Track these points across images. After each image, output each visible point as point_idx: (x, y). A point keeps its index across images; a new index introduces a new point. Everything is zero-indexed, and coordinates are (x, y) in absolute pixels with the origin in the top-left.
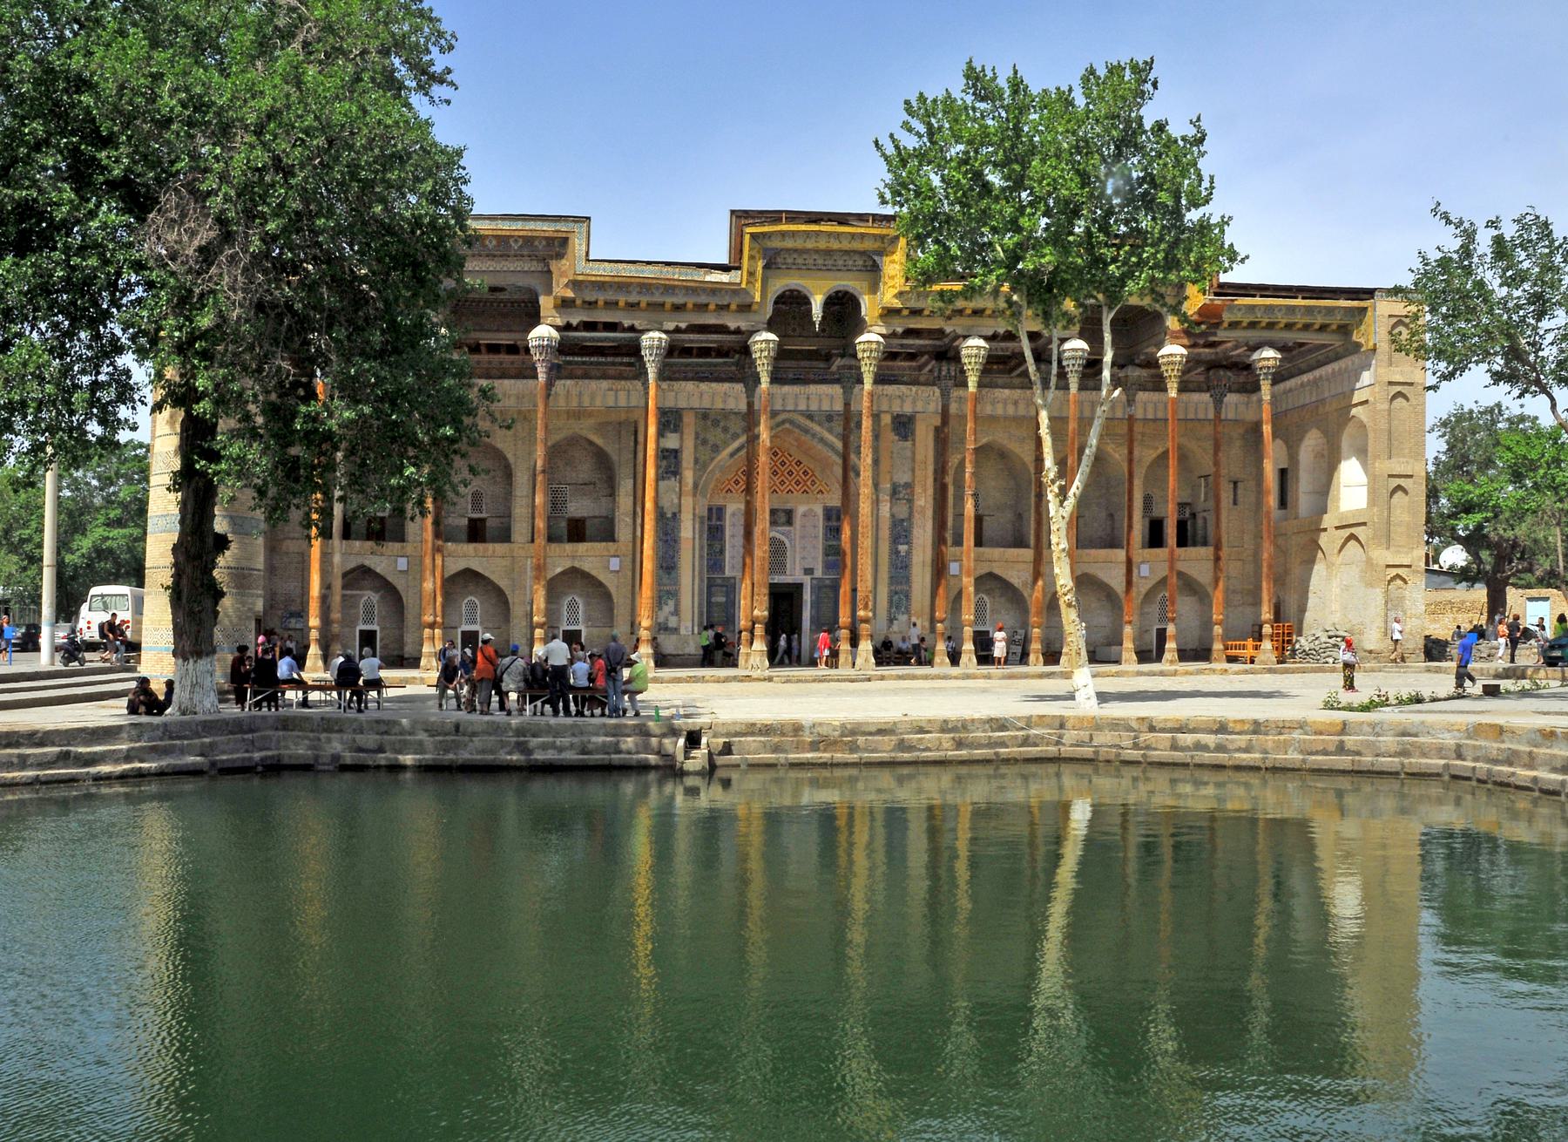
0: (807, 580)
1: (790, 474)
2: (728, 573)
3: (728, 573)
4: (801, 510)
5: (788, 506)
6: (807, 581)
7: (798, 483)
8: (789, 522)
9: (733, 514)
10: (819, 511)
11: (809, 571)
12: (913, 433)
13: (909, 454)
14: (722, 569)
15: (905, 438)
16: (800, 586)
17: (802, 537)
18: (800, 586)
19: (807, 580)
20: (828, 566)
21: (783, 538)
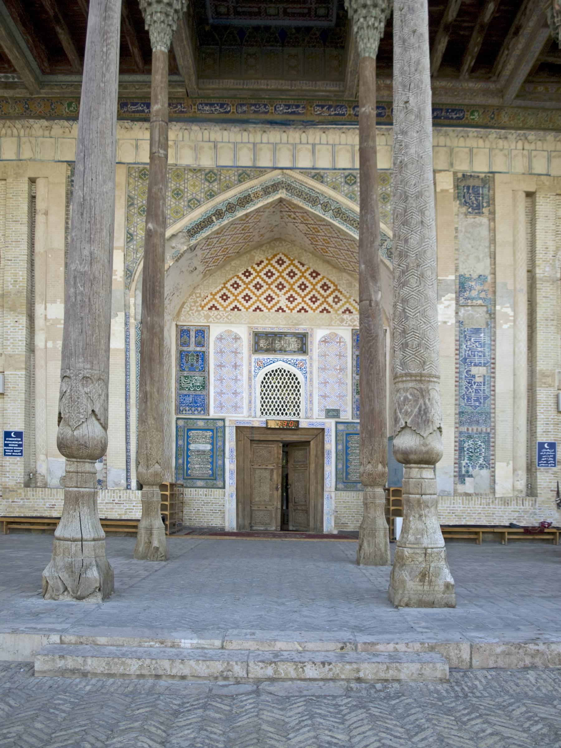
0: (330, 424)
1: (303, 287)
2: (213, 413)
3: (213, 413)
4: (319, 334)
5: (301, 329)
7: (314, 299)
8: (303, 350)
9: (220, 338)
10: (346, 335)
11: (333, 413)
12: (491, 202)
13: (485, 233)
14: (205, 408)
15: (477, 209)
17: (323, 369)
19: (330, 424)
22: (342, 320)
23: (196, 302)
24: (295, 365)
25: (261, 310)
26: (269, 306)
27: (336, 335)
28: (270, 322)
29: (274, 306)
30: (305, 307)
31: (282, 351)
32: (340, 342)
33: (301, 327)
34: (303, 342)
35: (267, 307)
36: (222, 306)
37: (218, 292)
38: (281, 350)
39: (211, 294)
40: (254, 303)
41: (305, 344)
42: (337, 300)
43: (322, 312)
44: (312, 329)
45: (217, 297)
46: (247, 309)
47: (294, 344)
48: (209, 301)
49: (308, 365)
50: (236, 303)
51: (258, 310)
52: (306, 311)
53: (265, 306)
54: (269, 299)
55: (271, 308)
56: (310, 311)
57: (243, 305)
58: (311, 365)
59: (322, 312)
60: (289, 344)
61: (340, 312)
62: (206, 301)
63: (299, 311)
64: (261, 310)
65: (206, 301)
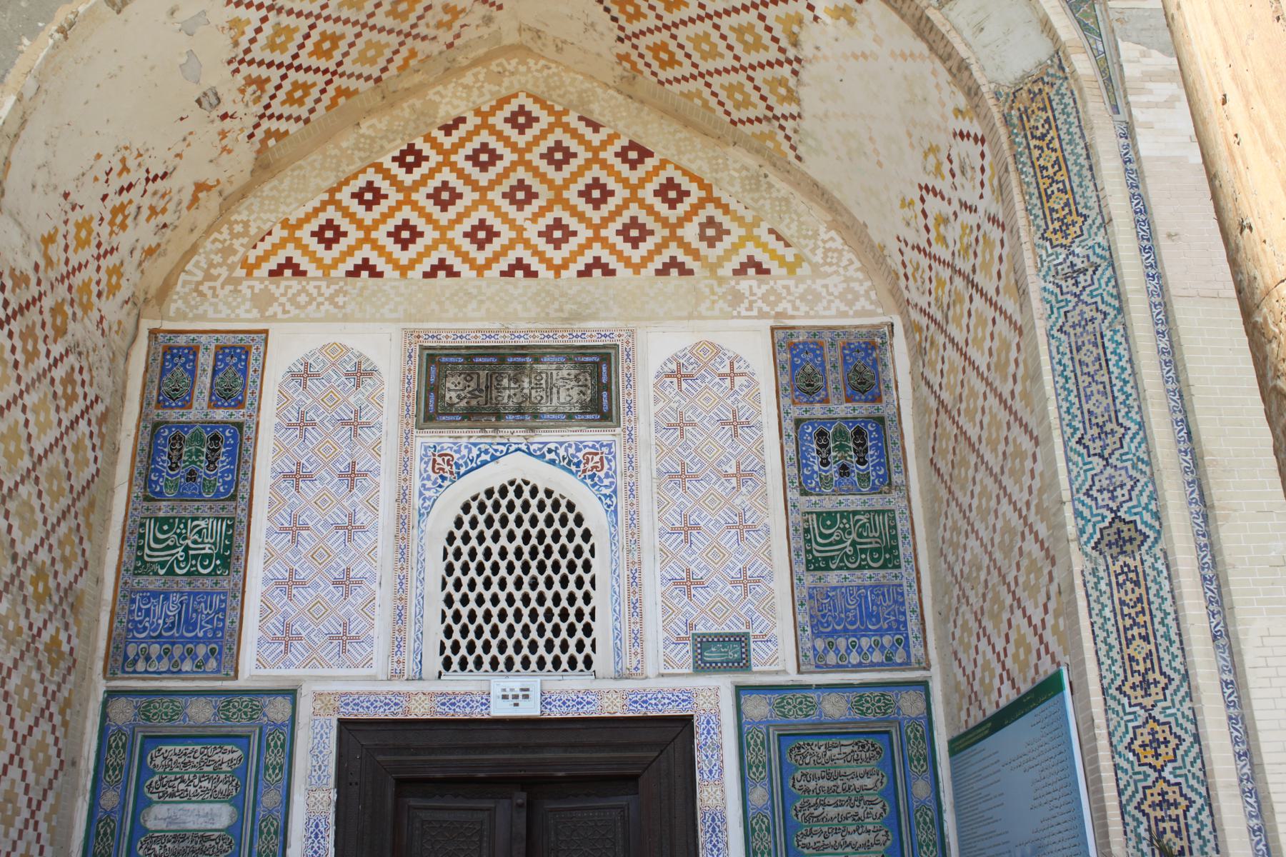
4: (653, 350)
6: (712, 699)
8: (600, 406)
16: (673, 734)
18: (673, 734)
20: (824, 623)
21: (568, 486)
22: (737, 298)
23: (228, 251)
24: (570, 465)
25: (451, 273)
26: (481, 257)
27: (718, 350)
28: (483, 311)
29: (496, 257)
30: (606, 257)
31: (528, 414)
32: (732, 375)
33: (591, 324)
34: (597, 381)
35: (472, 263)
36: (318, 262)
37: (308, 218)
38: (519, 411)
39: (285, 224)
40: (428, 250)
41: (608, 387)
42: (713, 232)
43: (663, 271)
44: (632, 333)
45: (304, 234)
46: (403, 270)
47: (568, 394)
48: (275, 248)
49: (620, 464)
50: (366, 251)
51: (442, 274)
52: (609, 272)
53: (465, 257)
54: (482, 234)
55: (488, 265)
56: (622, 271)
57: (390, 259)
58: (631, 462)
59: (663, 271)
60: (550, 388)
61: (727, 270)
62: (262, 247)
63: (586, 273)
64: (451, 273)
65: (262, 247)
